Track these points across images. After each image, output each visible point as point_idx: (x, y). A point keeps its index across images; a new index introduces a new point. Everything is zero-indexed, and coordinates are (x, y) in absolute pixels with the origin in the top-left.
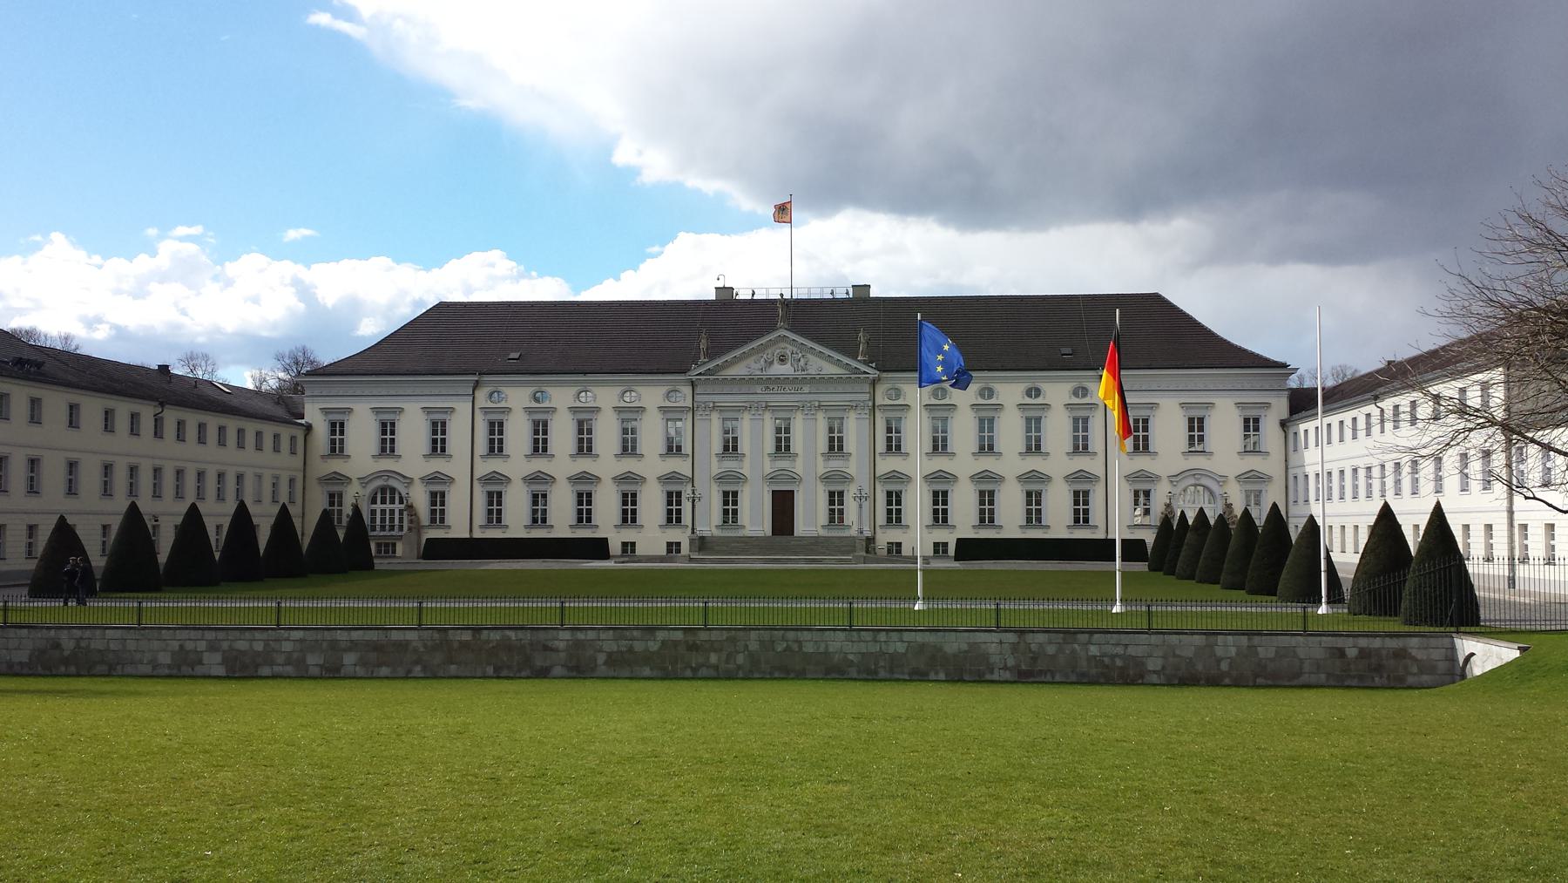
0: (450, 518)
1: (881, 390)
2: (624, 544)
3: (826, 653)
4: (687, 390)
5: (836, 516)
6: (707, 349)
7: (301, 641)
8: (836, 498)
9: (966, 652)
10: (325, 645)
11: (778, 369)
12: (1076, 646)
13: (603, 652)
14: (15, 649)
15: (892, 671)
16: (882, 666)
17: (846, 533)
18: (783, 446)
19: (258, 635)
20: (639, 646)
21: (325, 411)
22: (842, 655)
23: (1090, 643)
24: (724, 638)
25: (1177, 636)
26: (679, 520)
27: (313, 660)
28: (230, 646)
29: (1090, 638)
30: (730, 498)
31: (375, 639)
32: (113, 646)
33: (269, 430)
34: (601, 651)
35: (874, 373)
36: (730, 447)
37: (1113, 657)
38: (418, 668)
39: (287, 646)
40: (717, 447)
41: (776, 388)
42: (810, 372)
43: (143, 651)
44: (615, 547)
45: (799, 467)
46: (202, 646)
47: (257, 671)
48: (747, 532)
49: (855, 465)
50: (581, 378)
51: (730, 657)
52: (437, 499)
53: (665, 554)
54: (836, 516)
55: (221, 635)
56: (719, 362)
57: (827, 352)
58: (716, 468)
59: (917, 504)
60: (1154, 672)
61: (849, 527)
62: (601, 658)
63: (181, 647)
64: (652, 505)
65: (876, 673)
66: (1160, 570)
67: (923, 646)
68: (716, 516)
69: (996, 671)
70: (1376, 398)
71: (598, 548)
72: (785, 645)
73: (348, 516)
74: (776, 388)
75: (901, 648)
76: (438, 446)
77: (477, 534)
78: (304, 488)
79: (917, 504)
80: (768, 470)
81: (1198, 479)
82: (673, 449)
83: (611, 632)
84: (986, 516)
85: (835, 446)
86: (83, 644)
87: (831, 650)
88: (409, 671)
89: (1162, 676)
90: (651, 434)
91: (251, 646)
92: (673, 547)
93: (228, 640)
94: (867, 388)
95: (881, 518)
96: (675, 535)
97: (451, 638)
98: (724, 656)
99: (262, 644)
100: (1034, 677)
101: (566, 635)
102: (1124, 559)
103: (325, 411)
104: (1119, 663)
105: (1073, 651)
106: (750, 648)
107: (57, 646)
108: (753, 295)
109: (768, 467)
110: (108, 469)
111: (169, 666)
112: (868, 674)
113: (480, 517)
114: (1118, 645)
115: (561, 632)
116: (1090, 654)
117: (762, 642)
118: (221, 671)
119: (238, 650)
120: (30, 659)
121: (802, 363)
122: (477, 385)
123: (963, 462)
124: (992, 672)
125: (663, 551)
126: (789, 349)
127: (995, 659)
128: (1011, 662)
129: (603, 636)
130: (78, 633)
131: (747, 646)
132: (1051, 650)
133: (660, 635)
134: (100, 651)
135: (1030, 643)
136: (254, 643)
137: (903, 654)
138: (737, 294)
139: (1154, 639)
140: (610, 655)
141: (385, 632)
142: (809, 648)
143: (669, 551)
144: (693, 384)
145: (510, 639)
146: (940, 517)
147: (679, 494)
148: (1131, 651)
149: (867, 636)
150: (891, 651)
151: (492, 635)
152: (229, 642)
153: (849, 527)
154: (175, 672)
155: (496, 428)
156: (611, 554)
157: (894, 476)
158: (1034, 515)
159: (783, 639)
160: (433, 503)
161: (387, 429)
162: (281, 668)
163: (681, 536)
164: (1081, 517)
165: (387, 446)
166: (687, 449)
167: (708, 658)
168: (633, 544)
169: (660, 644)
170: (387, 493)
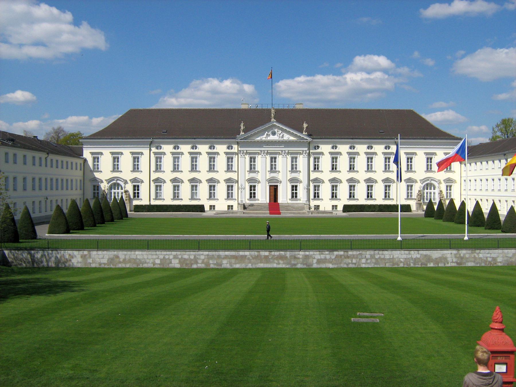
0: (141, 196)
1: (312, 146)
2: (211, 206)
3: (393, 258)
4: (235, 147)
5: (294, 195)
6: (243, 129)
7: (208, 255)
8: (294, 188)
9: (439, 257)
10: (216, 256)
11: (272, 138)
12: (475, 254)
13: (315, 259)
14: (101, 258)
15: (414, 264)
16: (412, 263)
17: (298, 202)
18: (273, 169)
19: (192, 253)
20: (328, 257)
21: (92, 153)
22: (398, 259)
23: (480, 253)
24: (358, 254)
25: (507, 250)
26: (232, 196)
27: (211, 262)
28: (182, 257)
29: (480, 252)
30: (252, 188)
31: (234, 254)
32: (138, 257)
33: (75, 160)
34: (314, 258)
35: (309, 139)
36: (252, 169)
37: (487, 258)
38: (250, 265)
39: (202, 257)
40: (248, 168)
41: (271, 145)
42: (284, 139)
43: (150, 259)
44: (207, 208)
45: (280, 176)
46: (171, 257)
47: (191, 266)
48: (259, 202)
49: (302, 176)
50: (193, 140)
51: (360, 259)
52: (136, 188)
53: (227, 210)
54: (294, 195)
55: (178, 253)
56: (249, 134)
57: (292, 131)
58: (248, 176)
59: (325, 190)
60: (500, 262)
61: (300, 200)
62: (315, 261)
63: (164, 257)
64: (221, 189)
65: (410, 265)
66: (433, 217)
67: (426, 256)
68: (248, 196)
69: (449, 263)
70: (505, 155)
71: (201, 208)
72: (379, 256)
73: (102, 195)
74: (271, 145)
75: (418, 256)
76: (136, 168)
77: (154, 203)
78: (84, 183)
79: (325, 190)
80: (268, 177)
81: (431, 181)
82: (229, 168)
83: (318, 252)
84: (351, 196)
85: (294, 169)
86: (127, 257)
87: (395, 257)
88: (246, 266)
89: (502, 263)
90: (221, 162)
91: (189, 257)
92: (230, 207)
93: (181, 255)
94: (307, 145)
95: (312, 196)
96: (230, 203)
97: (261, 254)
98: (358, 260)
99: (193, 256)
100: (461, 264)
101: (302, 253)
102: (401, 212)
103: (92, 153)
104: (489, 259)
105: (475, 256)
106: (367, 257)
107: (117, 257)
108: (257, 106)
109: (269, 176)
110: (34, 179)
111: (159, 264)
112: (407, 265)
113: (153, 196)
114: (488, 253)
115: (300, 252)
116: (480, 257)
117: (371, 255)
118: (178, 266)
119: (185, 259)
120: (108, 262)
121: (281, 135)
122: (151, 144)
123: (344, 175)
124: (448, 263)
125: (226, 209)
126: (276, 130)
127: (449, 259)
128: (454, 260)
129: (315, 253)
130: (125, 253)
131: (366, 256)
132: (467, 256)
133: (336, 253)
134: (133, 259)
135: (460, 254)
136: (191, 256)
137: (419, 258)
138: (250, 107)
139: (500, 251)
140: (318, 260)
141: (238, 252)
142: (387, 257)
143: (228, 209)
144: (238, 143)
145: (282, 254)
146: (334, 196)
147: (232, 186)
148: (493, 255)
149: (407, 252)
150: (415, 257)
151: (276, 253)
152: (181, 256)
153: (300, 200)
154: (162, 266)
155: (159, 159)
156: (205, 210)
157: (316, 180)
158: (369, 196)
159: (378, 254)
160: (134, 190)
161: (116, 159)
162: (200, 265)
163: (234, 204)
164: (387, 196)
165: (116, 168)
166: (235, 168)
167: (352, 261)
168: (214, 206)
169: (335, 255)
170: (116, 186)
